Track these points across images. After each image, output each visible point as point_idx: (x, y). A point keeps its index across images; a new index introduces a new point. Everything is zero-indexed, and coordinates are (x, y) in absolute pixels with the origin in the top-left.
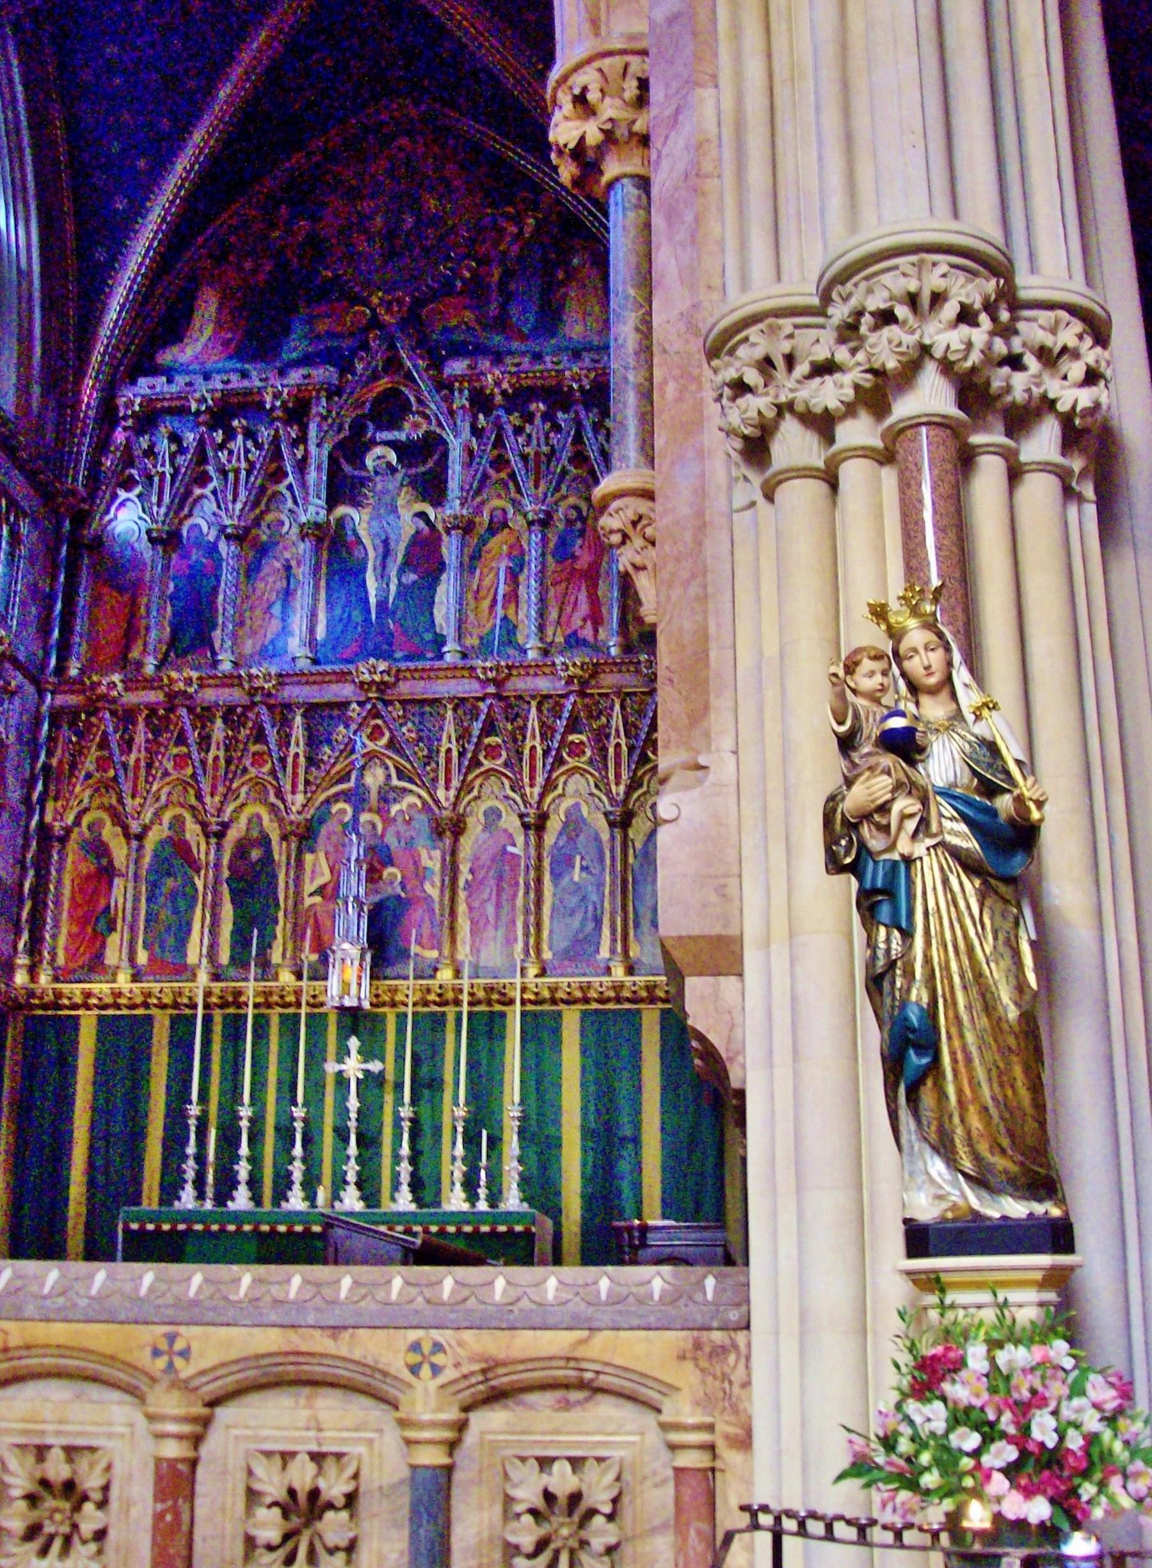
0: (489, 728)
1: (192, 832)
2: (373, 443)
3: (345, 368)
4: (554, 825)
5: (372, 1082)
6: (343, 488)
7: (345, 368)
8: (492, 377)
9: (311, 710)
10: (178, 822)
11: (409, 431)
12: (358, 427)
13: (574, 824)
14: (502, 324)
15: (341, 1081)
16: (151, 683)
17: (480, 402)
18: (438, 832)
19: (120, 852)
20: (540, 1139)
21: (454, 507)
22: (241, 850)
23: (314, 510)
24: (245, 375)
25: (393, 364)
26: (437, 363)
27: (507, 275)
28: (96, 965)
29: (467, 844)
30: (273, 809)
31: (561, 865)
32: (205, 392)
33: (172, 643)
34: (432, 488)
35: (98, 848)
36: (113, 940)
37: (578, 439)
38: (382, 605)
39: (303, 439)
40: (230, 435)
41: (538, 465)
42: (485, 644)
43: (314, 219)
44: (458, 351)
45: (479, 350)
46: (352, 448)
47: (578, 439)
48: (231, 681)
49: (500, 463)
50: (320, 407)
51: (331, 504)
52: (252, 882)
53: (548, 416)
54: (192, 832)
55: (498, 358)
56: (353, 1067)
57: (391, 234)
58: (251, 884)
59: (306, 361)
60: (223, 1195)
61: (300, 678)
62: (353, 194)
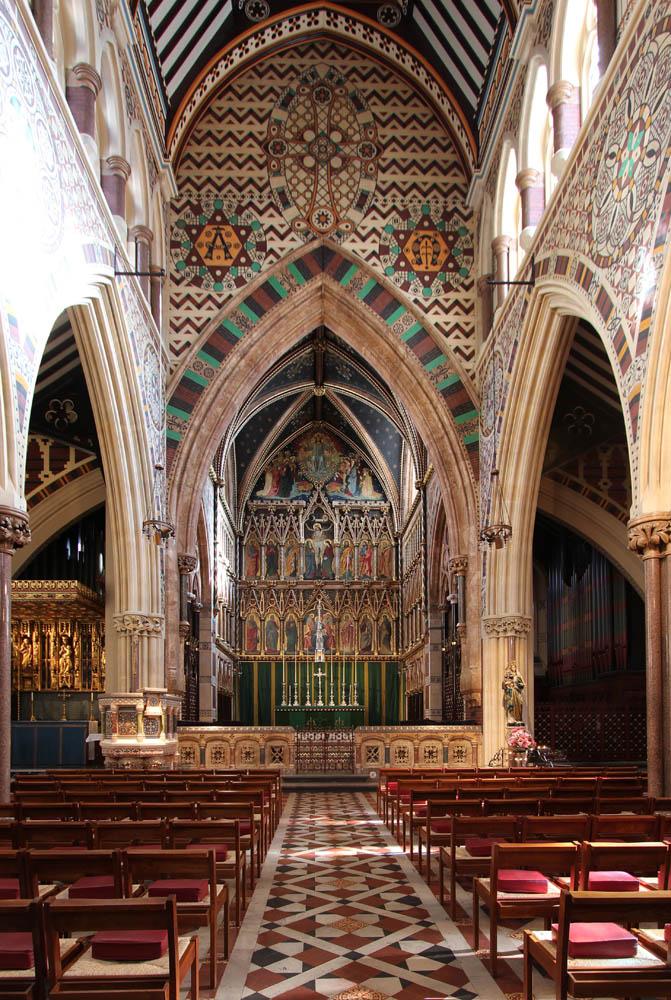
0: (346, 597)
1: (276, 619)
2: (314, 522)
3: (308, 502)
4: (361, 620)
5: (323, 677)
6: (308, 534)
7: (308, 502)
8: (347, 507)
9: (304, 591)
10: (272, 617)
11: (324, 520)
12: (311, 517)
13: (366, 619)
14: (347, 491)
15: (317, 678)
16: (263, 583)
17: (342, 513)
18: (334, 622)
19: (259, 625)
20: (360, 690)
21: (336, 541)
22: (289, 623)
23: (303, 540)
24: (282, 501)
25: (319, 500)
26: (330, 502)
27: (348, 477)
28: (254, 651)
29: (342, 624)
30: (296, 616)
31: (363, 630)
32: (272, 507)
33: (268, 572)
34: (331, 535)
35: (254, 623)
36: (259, 644)
37: (366, 524)
38: (319, 565)
39: (297, 521)
40: (279, 518)
41: (356, 531)
42: (344, 577)
43: (296, 455)
44: (336, 498)
45: (341, 499)
46: (310, 523)
47: (366, 524)
48: (283, 583)
49: (347, 529)
50: (302, 512)
51: (306, 538)
52: (291, 631)
53: (359, 518)
54: (276, 619)
55: (346, 501)
56: (320, 675)
57: (317, 462)
58: (291, 631)
59: (297, 498)
60: (293, 703)
61: (302, 583)
62: (306, 450)
